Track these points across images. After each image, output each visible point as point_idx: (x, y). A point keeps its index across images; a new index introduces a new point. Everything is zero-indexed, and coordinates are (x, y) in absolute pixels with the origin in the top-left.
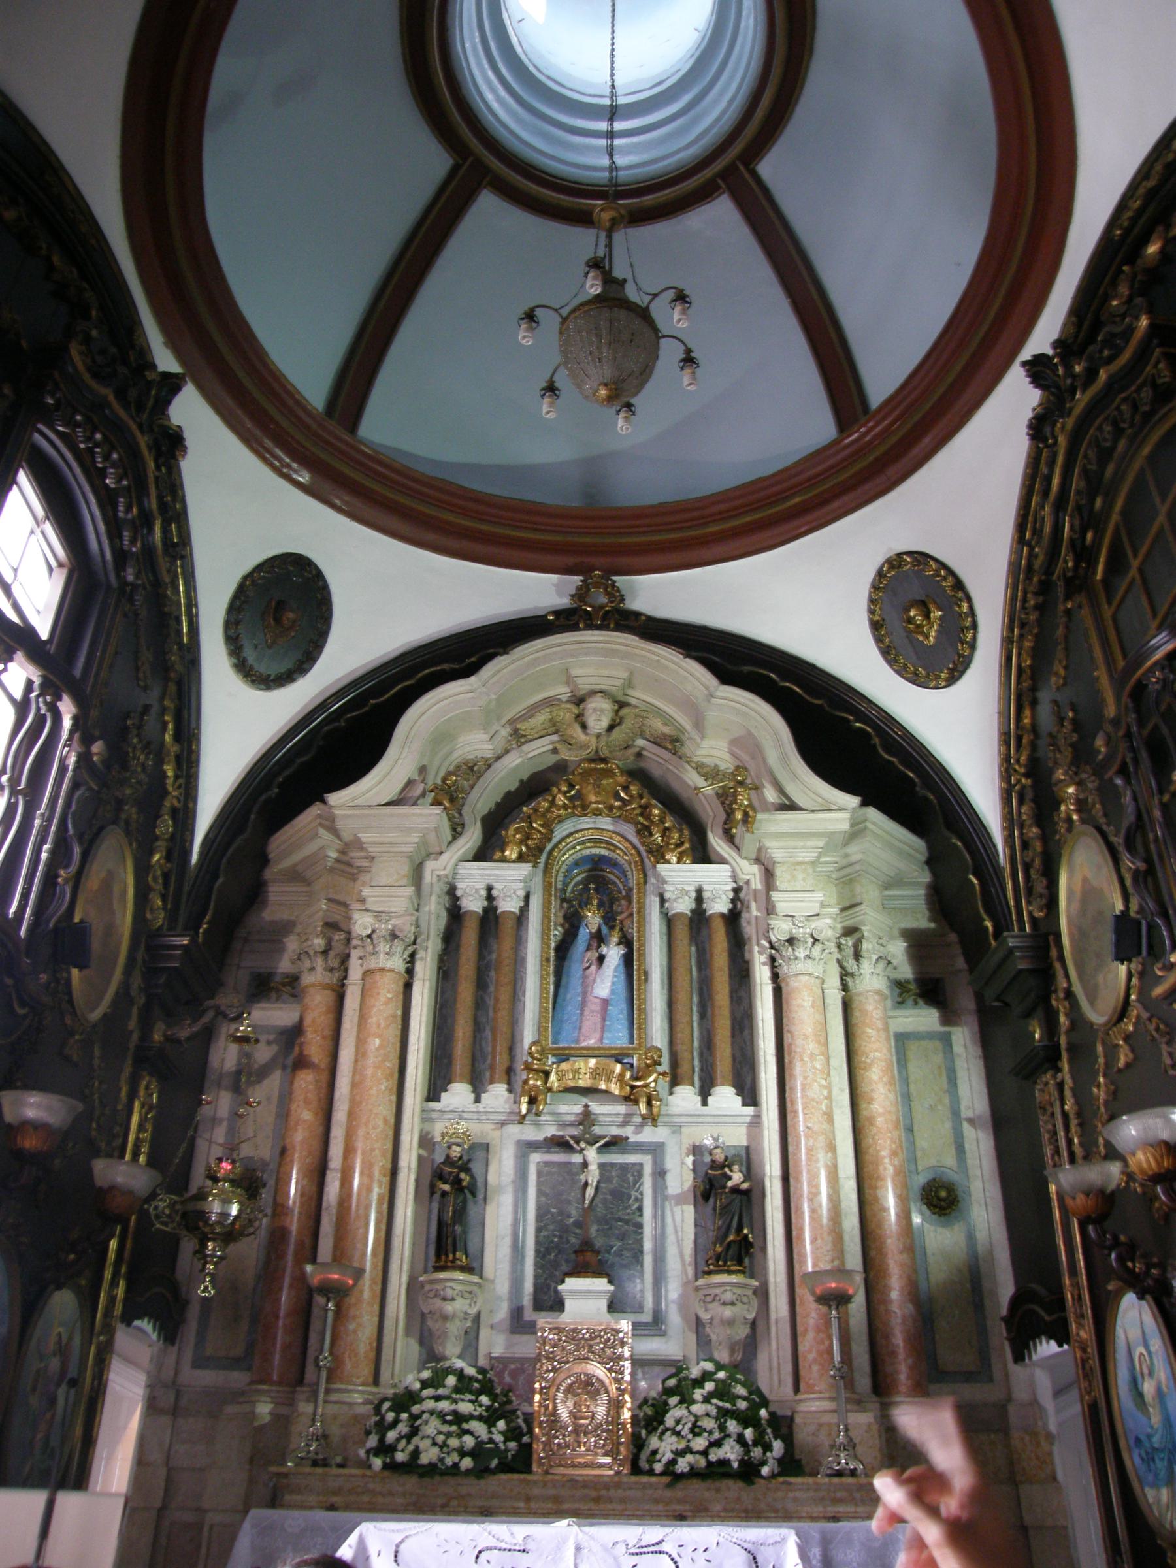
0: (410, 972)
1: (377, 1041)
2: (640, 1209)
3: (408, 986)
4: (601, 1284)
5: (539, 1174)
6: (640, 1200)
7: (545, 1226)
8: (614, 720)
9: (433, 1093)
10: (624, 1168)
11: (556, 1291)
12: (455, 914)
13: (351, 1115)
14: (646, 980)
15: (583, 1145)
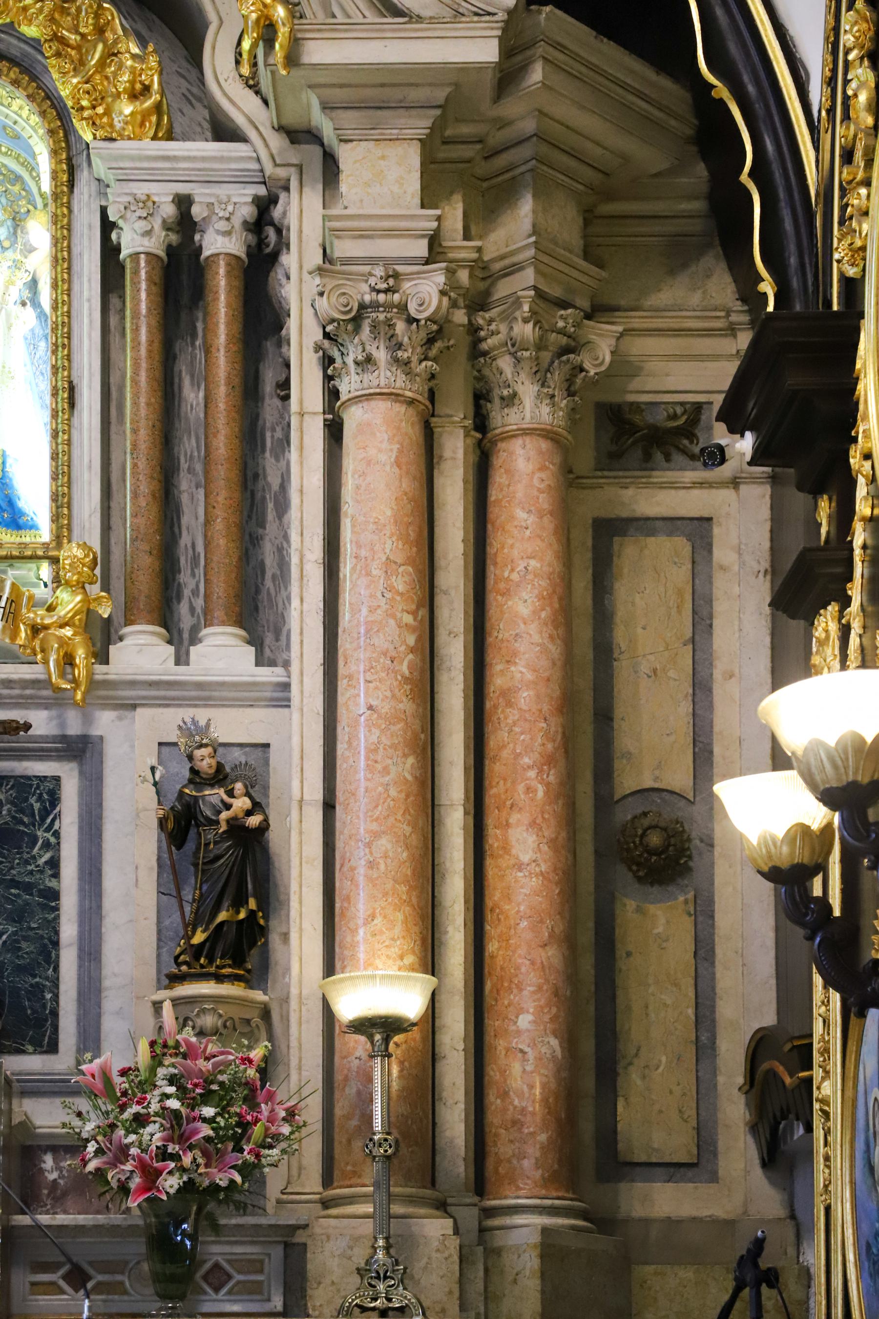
2: (54, 864)
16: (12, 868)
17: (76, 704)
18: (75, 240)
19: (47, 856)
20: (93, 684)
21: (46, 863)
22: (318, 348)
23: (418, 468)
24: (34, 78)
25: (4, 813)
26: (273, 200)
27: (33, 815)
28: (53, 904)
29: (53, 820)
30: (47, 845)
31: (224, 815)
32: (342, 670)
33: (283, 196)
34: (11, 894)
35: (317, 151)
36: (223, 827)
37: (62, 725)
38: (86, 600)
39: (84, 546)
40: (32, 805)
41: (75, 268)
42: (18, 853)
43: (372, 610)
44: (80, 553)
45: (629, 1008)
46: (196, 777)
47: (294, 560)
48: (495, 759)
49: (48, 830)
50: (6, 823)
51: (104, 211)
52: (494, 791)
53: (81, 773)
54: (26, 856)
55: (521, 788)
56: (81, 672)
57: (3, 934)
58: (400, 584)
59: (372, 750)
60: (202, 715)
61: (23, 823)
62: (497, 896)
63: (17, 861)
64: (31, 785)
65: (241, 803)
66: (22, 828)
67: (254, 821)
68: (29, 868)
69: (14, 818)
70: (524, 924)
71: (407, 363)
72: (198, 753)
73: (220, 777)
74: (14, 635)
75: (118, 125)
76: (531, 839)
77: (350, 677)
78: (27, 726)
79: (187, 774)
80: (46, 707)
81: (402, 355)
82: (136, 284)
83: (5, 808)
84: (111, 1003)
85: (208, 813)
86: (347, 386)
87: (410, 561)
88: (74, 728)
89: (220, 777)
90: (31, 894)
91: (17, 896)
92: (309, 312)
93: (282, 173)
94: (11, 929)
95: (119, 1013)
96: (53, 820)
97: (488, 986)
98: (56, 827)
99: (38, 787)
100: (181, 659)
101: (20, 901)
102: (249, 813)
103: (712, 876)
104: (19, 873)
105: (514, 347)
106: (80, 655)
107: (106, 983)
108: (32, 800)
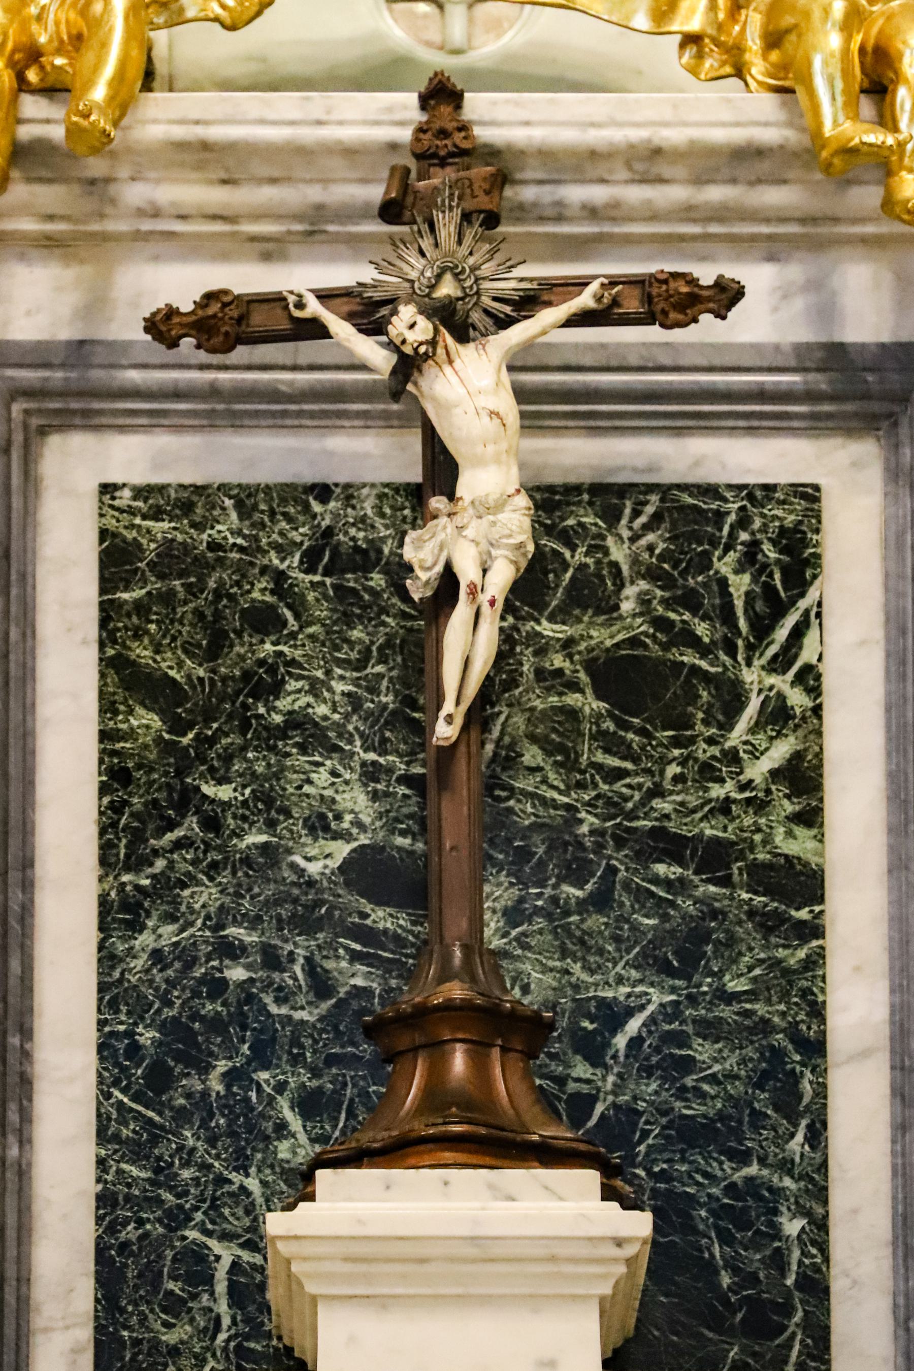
16: (657, 792)
21: (775, 774)
25: (627, 606)
27: (727, 614)
28: (803, 914)
29: (798, 633)
34: (656, 880)
40: (723, 583)
42: (676, 742)
49: (780, 664)
50: (634, 642)
54: (704, 751)
57: (630, 1013)
61: (694, 642)
63: (673, 770)
64: (720, 516)
66: (689, 658)
68: (717, 791)
69: (661, 624)
83: (630, 591)
90: (726, 881)
91: (679, 886)
94: (657, 998)
96: (798, 633)
98: (808, 655)
99: (743, 522)
101: (688, 905)
104: (683, 810)
108: (725, 565)
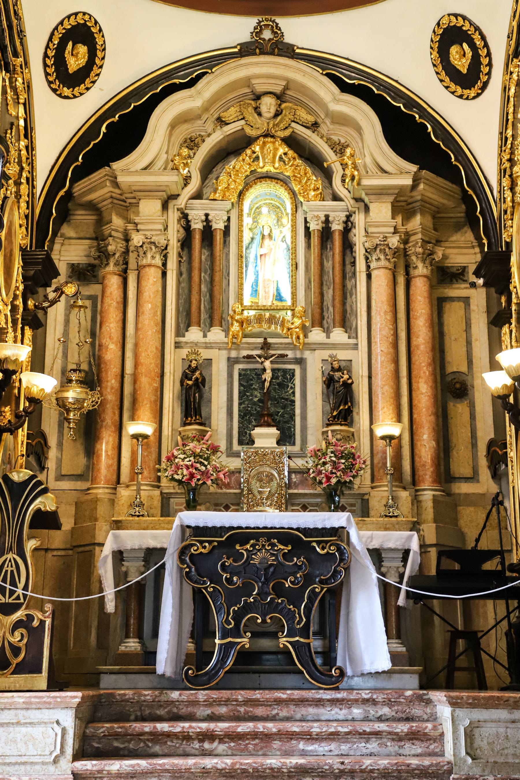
0: (164, 265)
1: (150, 305)
2: (294, 393)
3: (164, 274)
4: (274, 431)
5: (240, 375)
6: (293, 388)
7: (244, 402)
8: (277, 110)
9: (179, 333)
10: (285, 371)
11: (250, 435)
12: (187, 229)
13: (136, 345)
14: (297, 268)
15: (263, 359)
17: (299, 349)
18: (297, 226)
19: (292, 391)
20: (304, 344)
22: (364, 255)
23: (392, 287)
24: (286, 184)
26: (351, 216)
30: (292, 388)
31: (342, 380)
32: (373, 340)
33: (353, 215)
35: (363, 204)
36: (341, 383)
37: (296, 355)
38: (302, 321)
39: (302, 307)
41: (297, 233)
43: (381, 324)
44: (301, 309)
45: (452, 433)
46: (333, 369)
47: (359, 310)
48: (414, 364)
51: (305, 219)
52: (414, 373)
53: (301, 368)
55: (422, 372)
56: (301, 341)
58: (389, 317)
59: (382, 362)
60: (334, 352)
62: (416, 402)
65: (346, 377)
67: (350, 381)
70: (424, 410)
71: (389, 259)
72: (334, 363)
73: (339, 369)
74: (283, 331)
75: (310, 197)
76: (425, 386)
77: (376, 342)
78: (287, 355)
79: (330, 368)
80: (291, 350)
81: (388, 257)
82: (314, 237)
84: (310, 432)
85: (337, 379)
86: (373, 265)
87: (391, 311)
88: (298, 356)
89: (339, 369)
92: (361, 245)
93: (354, 209)
95: (312, 434)
97: (414, 427)
100: (328, 337)
102: (348, 379)
103: (474, 396)
105: (417, 254)
106: (301, 336)
107: (308, 426)
